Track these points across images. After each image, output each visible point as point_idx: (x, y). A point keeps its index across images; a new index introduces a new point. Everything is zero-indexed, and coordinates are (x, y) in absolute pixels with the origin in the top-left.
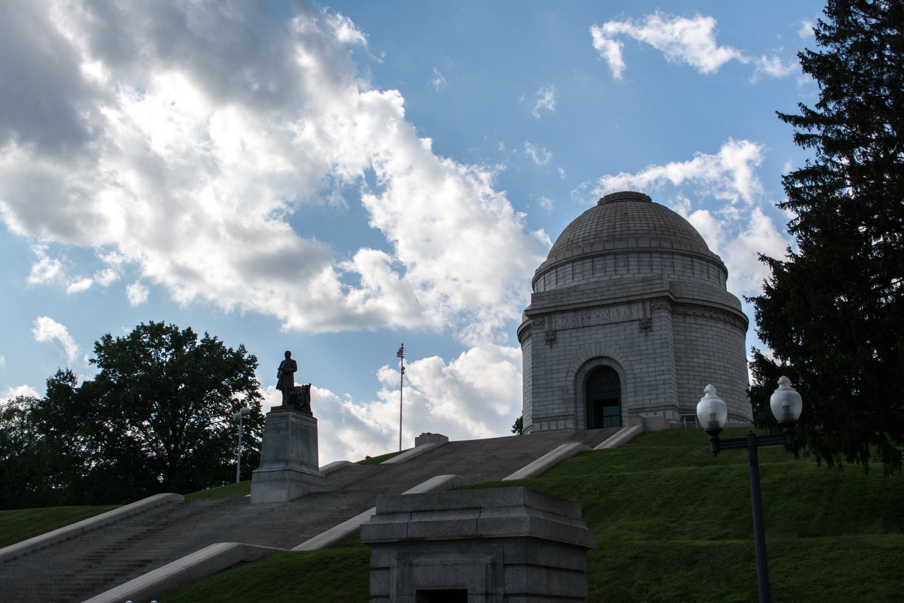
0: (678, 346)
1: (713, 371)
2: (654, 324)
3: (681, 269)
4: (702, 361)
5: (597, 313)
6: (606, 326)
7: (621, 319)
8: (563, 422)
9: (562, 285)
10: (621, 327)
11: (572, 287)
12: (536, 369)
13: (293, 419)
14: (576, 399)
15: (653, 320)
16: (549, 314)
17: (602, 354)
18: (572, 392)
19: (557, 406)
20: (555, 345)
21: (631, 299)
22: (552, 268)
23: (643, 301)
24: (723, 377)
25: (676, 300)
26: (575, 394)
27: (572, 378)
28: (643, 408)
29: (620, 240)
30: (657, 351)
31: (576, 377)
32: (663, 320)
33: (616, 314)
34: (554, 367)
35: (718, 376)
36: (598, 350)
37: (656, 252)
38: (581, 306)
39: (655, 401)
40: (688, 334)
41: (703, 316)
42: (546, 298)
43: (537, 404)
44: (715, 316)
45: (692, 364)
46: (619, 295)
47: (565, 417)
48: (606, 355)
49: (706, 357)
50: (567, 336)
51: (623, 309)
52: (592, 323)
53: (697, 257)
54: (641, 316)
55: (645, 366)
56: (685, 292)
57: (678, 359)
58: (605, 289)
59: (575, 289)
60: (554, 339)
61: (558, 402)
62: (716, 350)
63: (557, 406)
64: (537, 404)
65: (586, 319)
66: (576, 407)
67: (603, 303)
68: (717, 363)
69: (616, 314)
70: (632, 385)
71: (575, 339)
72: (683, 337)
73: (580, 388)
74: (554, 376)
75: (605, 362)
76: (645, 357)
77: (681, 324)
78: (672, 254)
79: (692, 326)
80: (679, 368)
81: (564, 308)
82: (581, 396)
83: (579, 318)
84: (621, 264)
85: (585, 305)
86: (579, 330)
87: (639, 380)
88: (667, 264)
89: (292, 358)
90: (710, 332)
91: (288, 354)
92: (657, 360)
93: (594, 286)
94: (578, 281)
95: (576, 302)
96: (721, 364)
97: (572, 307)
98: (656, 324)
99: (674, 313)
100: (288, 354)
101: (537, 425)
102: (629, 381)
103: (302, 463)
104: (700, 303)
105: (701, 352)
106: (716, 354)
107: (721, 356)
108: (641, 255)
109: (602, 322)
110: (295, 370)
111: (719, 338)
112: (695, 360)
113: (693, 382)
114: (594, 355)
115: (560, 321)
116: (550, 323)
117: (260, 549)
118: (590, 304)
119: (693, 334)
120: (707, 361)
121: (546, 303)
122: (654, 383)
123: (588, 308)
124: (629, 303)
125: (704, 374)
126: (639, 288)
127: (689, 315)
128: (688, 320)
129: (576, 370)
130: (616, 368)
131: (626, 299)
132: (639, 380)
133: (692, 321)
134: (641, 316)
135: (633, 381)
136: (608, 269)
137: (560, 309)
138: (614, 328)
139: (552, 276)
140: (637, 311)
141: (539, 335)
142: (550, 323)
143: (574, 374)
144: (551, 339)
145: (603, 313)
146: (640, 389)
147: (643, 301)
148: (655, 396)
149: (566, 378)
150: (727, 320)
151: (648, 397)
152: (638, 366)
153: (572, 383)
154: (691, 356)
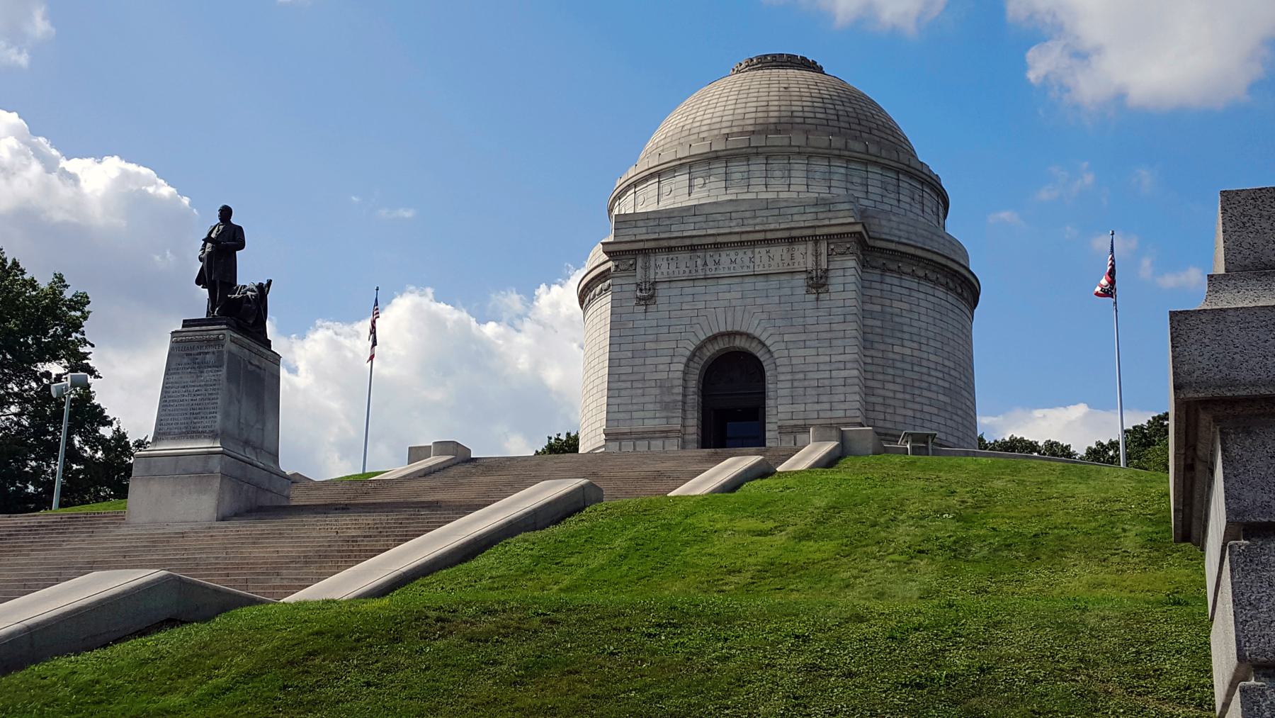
0: (869, 322)
1: (925, 370)
2: (832, 281)
3: (879, 191)
4: (908, 352)
5: (732, 253)
6: (747, 280)
7: (773, 269)
8: (659, 443)
9: (667, 203)
10: (774, 282)
11: (689, 208)
12: (616, 348)
13: (234, 348)
14: (684, 403)
15: (831, 274)
16: (645, 252)
17: (737, 328)
18: (680, 390)
19: (651, 414)
20: (652, 308)
21: (795, 233)
22: (652, 176)
23: (816, 239)
24: (941, 383)
25: (871, 243)
26: (684, 395)
27: (681, 367)
29: (778, 132)
31: (687, 365)
32: (846, 274)
33: (765, 258)
34: (648, 346)
35: (933, 380)
36: (729, 320)
37: (839, 157)
38: (704, 241)
39: (829, 414)
40: (887, 302)
41: (913, 274)
42: (640, 224)
43: (615, 408)
44: (933, 276)
45: (891, 355)
46: (772, 227)
47: (665, 434)
48: (744, 329)
49: (915, 345)
50: (677, 292)
51: (778, 252)
52: (721, 272)
53: (907, 173)
54: (810, 264)
55: (813, 352)
56: (886, 230)
57: (867, 342)
58: (748, 214)
59: (694, 211)
60: (652, 296)
61: (651, 407)
62: (931, 335)
63: (651, 414)
64: (615, 408)
65: (711, 264)
66: (684, 419)
67: (744, 237)
68: (932, 357)
69: (764, 259)
70: (789, 385)
71: (690, 298)
72: (878, 308)
73: (693, 384)
74: (649, 361)
75: (739, 343)
76: (814, 336)
77: (877, 285)
78: (866, 163)
79: (895, 289)
80: (869, 360)
81: (673, 243)
82: (693, 399)
83: (700, 262)
84: (778, 174)
85: (711, 240)
86: (697, 283)
87: (801, 376)
88: (856, 180)
89: (234, 220)
90: (923, 303)
91: (226, 213)
92: (835, 343)
94: (700, 196)
95: (695, 233)
96: (940, 360)
97: (688, 242)
98: (836, 282)
99: (864, 265)
100: (226, 213)
101: (614, 446)
102: (782, 377)
103: (247, 443)
104: (912, 251)
105: (906, 336)
106: (932, 343)
107: (939, 345)
108: (813, 161)
109: (739, 272)
110: (241, 245)
111: (938, 316)
112: (897, 349)
113: (891, 386)
114: (723, 329)
115: (665, 264)
116: (646, 268)
117: (217, 591)
118: (720, 239)
119: (895, 304)
120: (916, 353)
121: (641, 233)
122: (827, 382)
123: (718, 246)
124: (791, 240)
125: (908, 374)
126: (810, 217)
127: (892, 271)
128: (888, 280)
129: (688, 353)
130: (760, 354)
131: (786, 234)
132: (801, 376)
133: (896, 282)
134: (810, 264)
135: (789, 377)
136: (753, 181)
137: (665, 244)
138: (761, 284)
139: (652, 186)
140: (804, 257)
141: (625, 288)
142: (646, 268)
143: (684, 360)
144: (647, 296)
145: (743, 256)
146: (801, 391)
147: (816, 239)
148: (827, 406)
149: (672, 367)
150: (951, 285)
151: (817, 407)
152: (801, 352)
153: (680, 375)
154: (890, 341)
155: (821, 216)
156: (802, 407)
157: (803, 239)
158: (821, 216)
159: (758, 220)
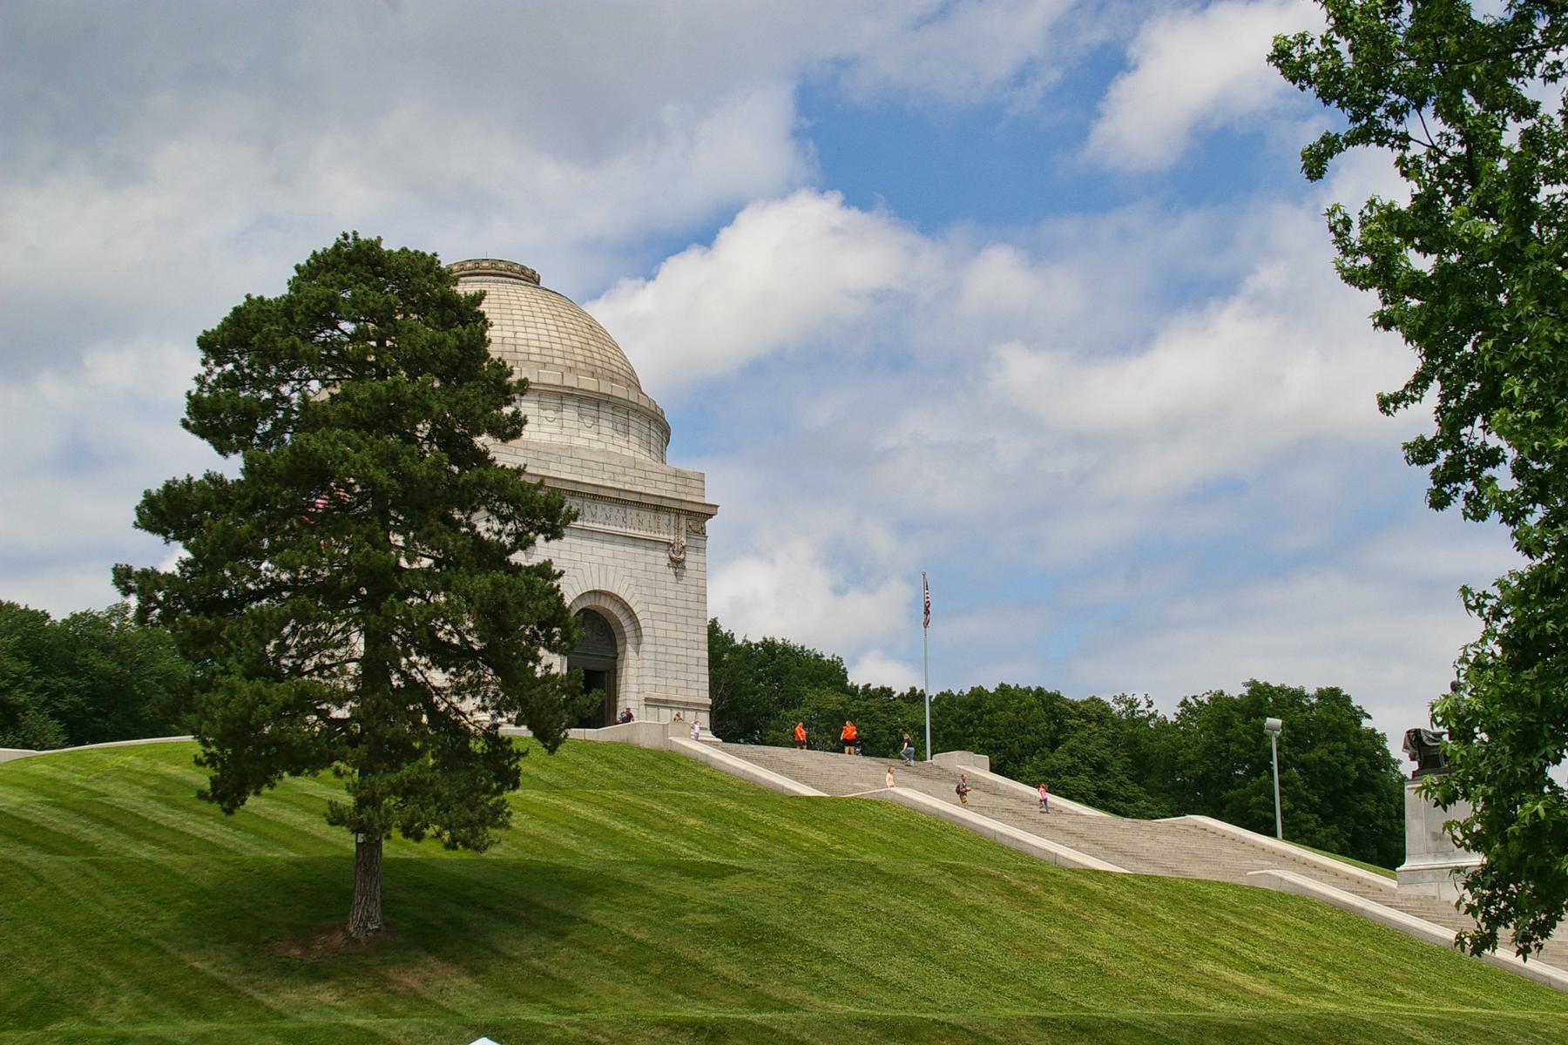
23: (678, 512)
28: (667, 701)
30: (690, 605)
55: (672, 627)
58: (619, 470)
75: (604, 603)
76: (673, 611)
87: (662, 649)
93: (601, 459)
122: (684, 660)
123: (595, 497)
124: (658, 509)
132: (662, 649)
146: (662, 665)
147: (678, 512)
151: (675, 683)
152: (664, 625)
155: (680, 489)
156: (663, 681)
157: (668, 510)
158: (680, 489)
159: (627, 479)
